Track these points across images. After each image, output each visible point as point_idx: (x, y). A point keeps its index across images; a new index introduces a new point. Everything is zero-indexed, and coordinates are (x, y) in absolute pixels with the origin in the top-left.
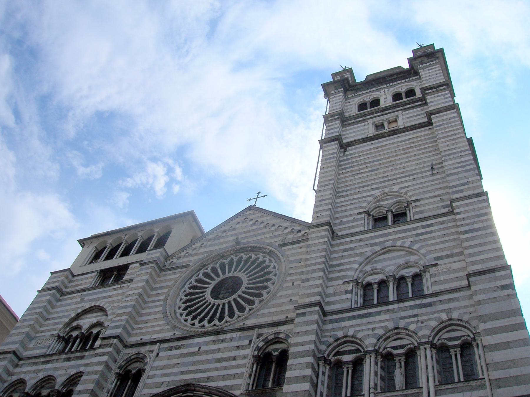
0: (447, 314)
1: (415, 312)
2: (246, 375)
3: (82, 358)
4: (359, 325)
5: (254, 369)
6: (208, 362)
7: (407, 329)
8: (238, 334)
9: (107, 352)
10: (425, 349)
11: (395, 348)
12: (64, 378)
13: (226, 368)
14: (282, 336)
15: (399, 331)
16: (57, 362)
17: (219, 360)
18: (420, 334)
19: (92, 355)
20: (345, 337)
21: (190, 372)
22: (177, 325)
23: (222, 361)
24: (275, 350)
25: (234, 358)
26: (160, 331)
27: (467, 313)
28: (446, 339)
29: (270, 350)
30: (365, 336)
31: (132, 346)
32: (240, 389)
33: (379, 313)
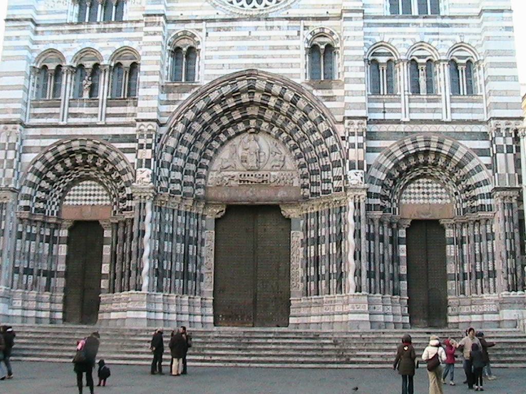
0: (461, 36)
1: (436, 30)
2: (303, 66)
3: (120, 30)
4: (392, 33)
5: (308, 60)
6: (263, 48)
7: (430, 45)
8: (286, 23)
9: (158, 32)
10: (444, 65)
11: (419, 57)
12: (110, 53)
13: (281, 56)
14: (327, 31)
15: (423, 44)
16: (89, 32)
17: (273, 48)
18: (440, 51)
19: (131, 28)
20: (381, 42)
21: (248, 57)
22: (217, 4)
23: (276, 49)
24: (322, 43)
25: (287, 48)
26: (201, 8)
27: (474, 40)
28: (457, 57)
29: (317, 43)
30: (398, 44)
31: (174, 22)
32: (300, 78)
33: (408, 25)
